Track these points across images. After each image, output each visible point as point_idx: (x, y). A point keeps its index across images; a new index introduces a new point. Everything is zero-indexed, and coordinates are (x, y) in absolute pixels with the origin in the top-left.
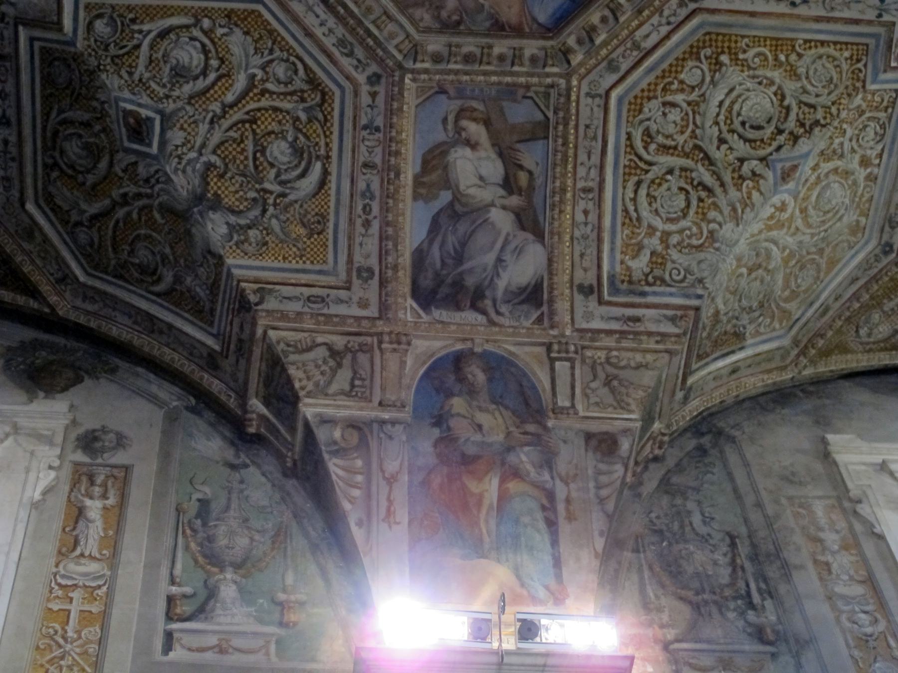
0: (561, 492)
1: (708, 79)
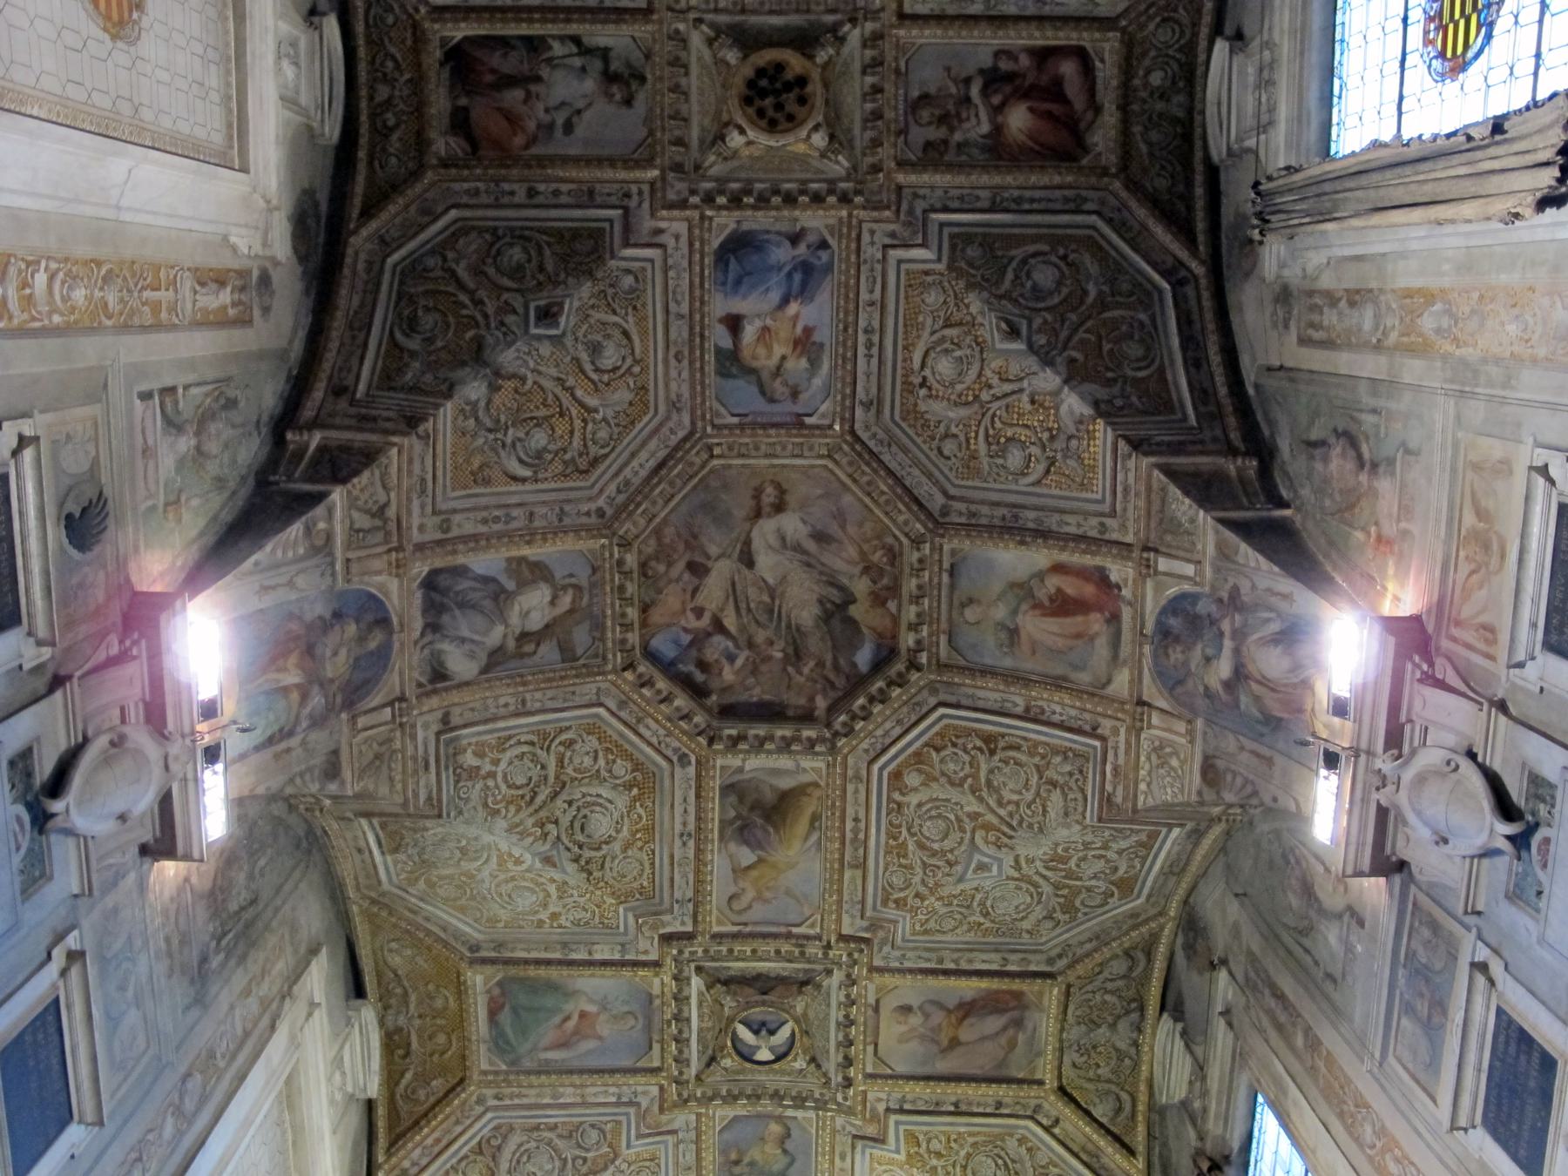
0: (294, 742)
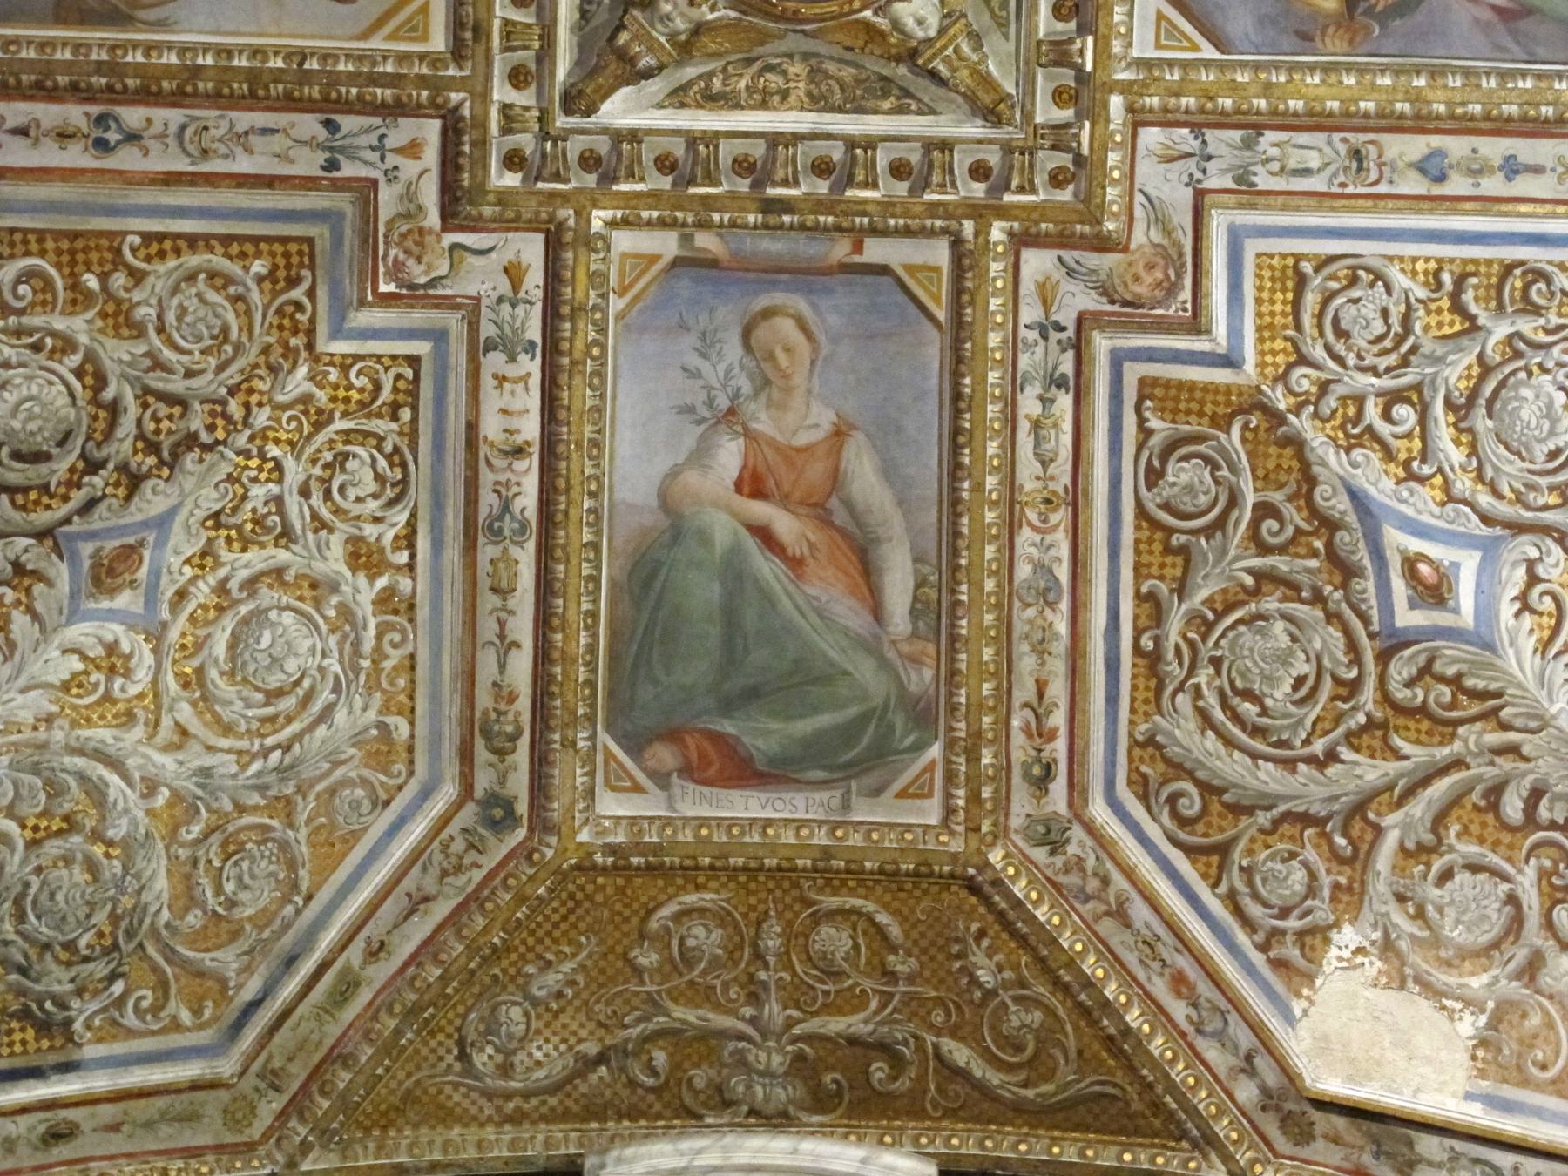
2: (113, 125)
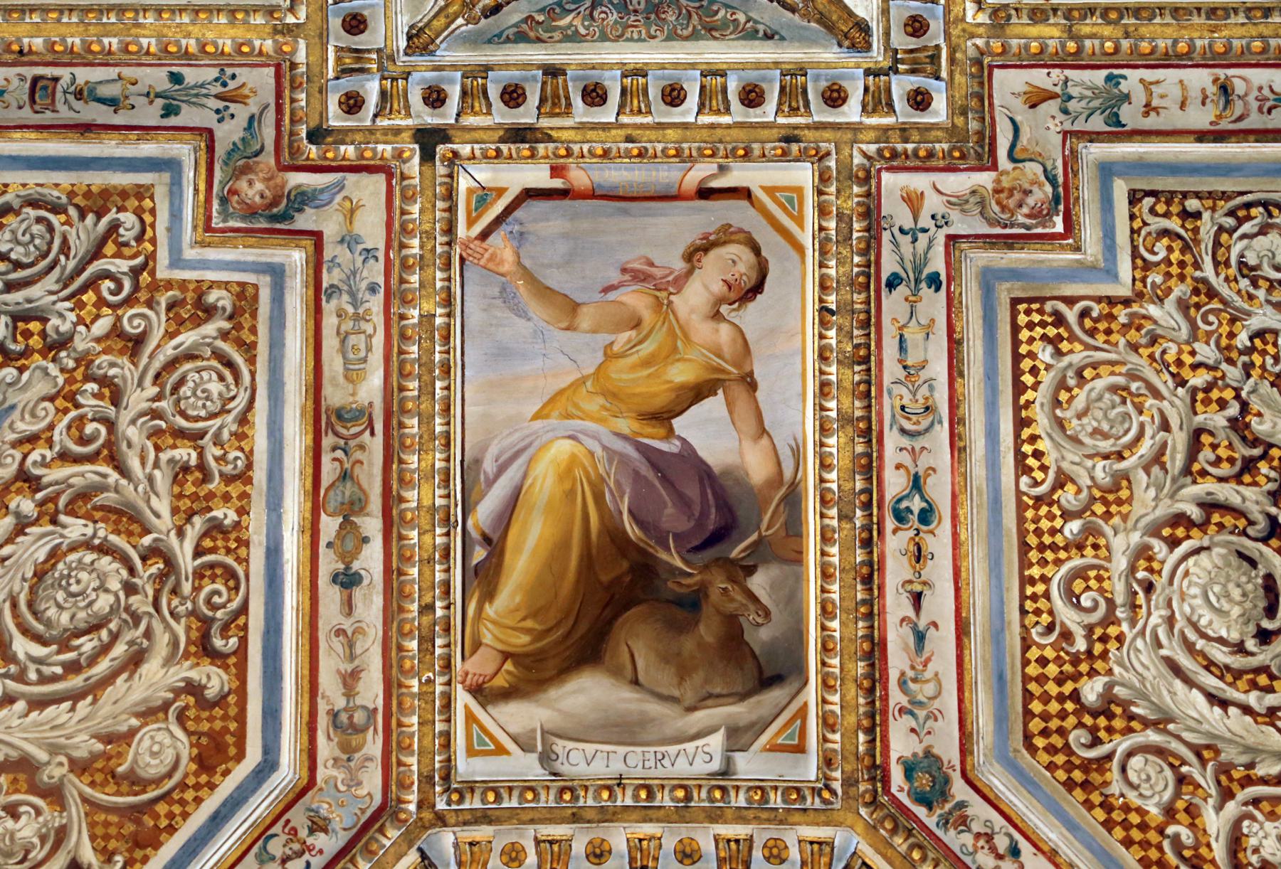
1: (1153, 737)
2: (904, 505)
